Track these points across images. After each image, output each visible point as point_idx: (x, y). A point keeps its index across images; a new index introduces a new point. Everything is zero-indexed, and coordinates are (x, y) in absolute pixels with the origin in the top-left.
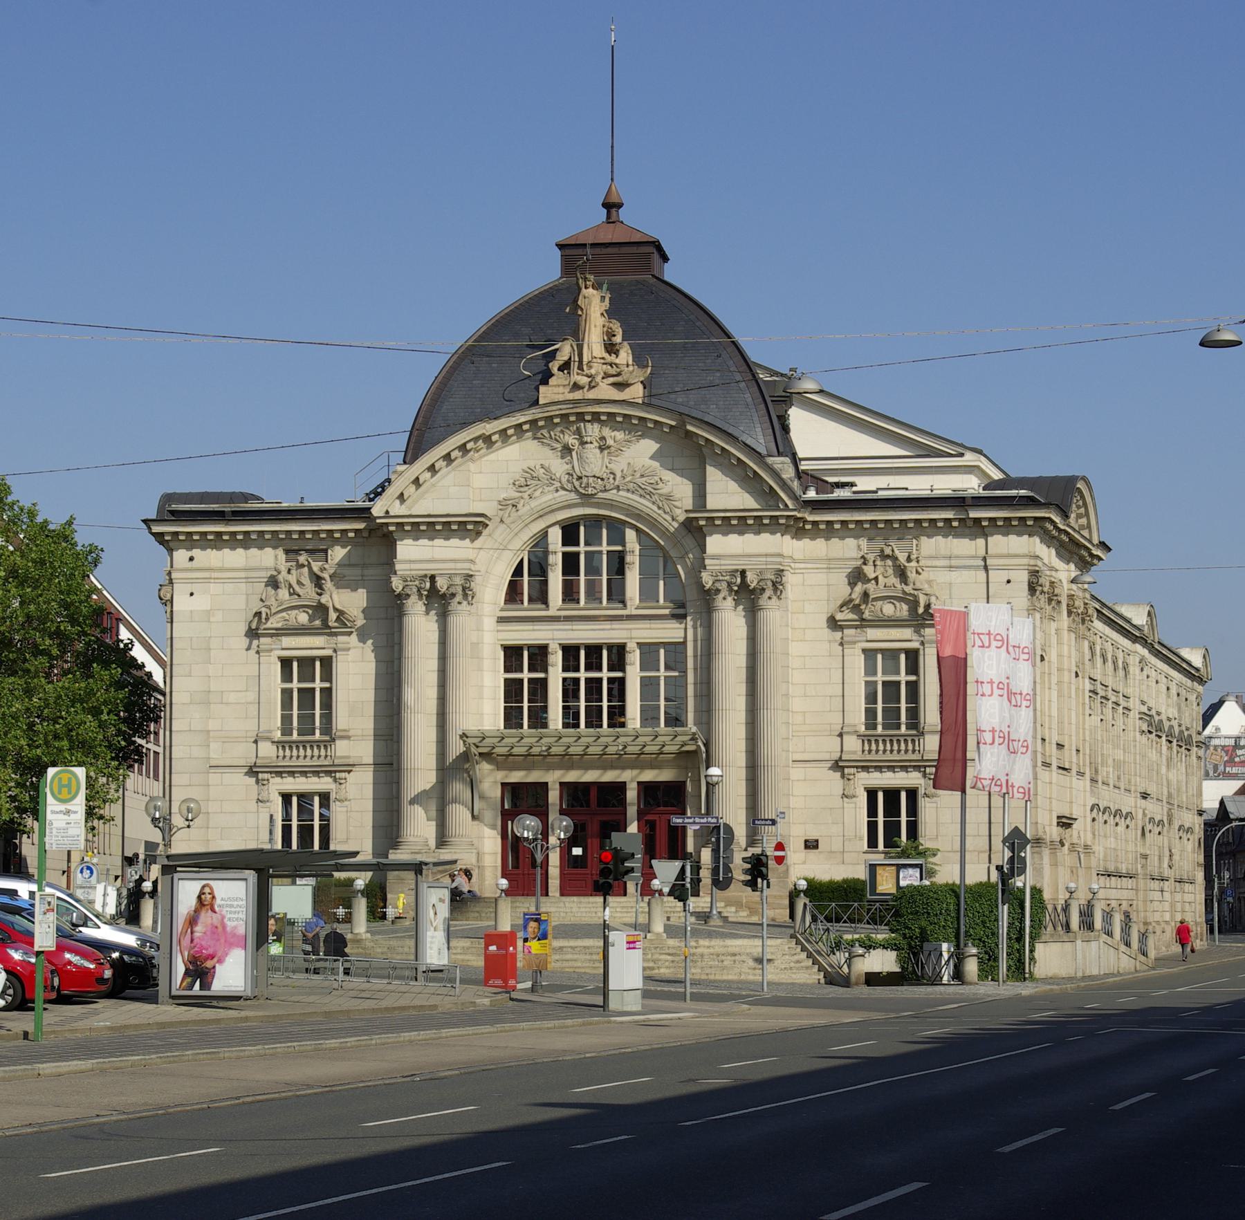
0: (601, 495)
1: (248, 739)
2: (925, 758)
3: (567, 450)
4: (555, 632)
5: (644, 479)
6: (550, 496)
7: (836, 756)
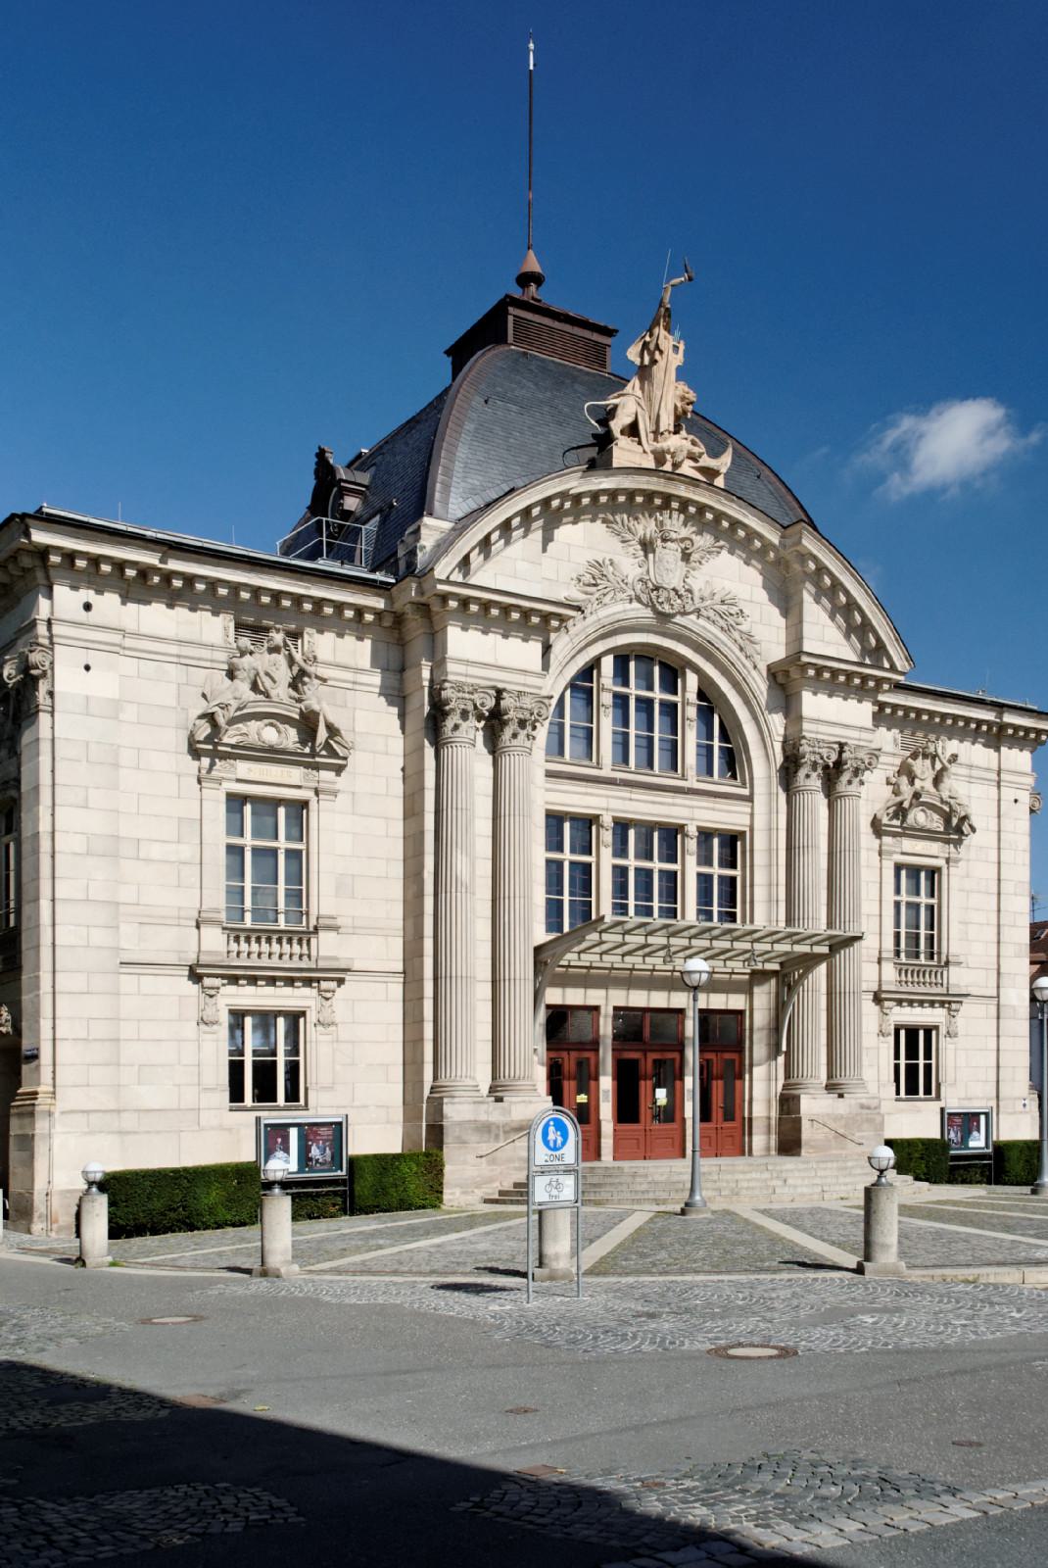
0: (678, 619)
1: (182, 922)
2: (950, 992)
3: (647, 546)
4: (610, 800)
5: (725, 607)
6: (619, 607)
7: (876, 988)
